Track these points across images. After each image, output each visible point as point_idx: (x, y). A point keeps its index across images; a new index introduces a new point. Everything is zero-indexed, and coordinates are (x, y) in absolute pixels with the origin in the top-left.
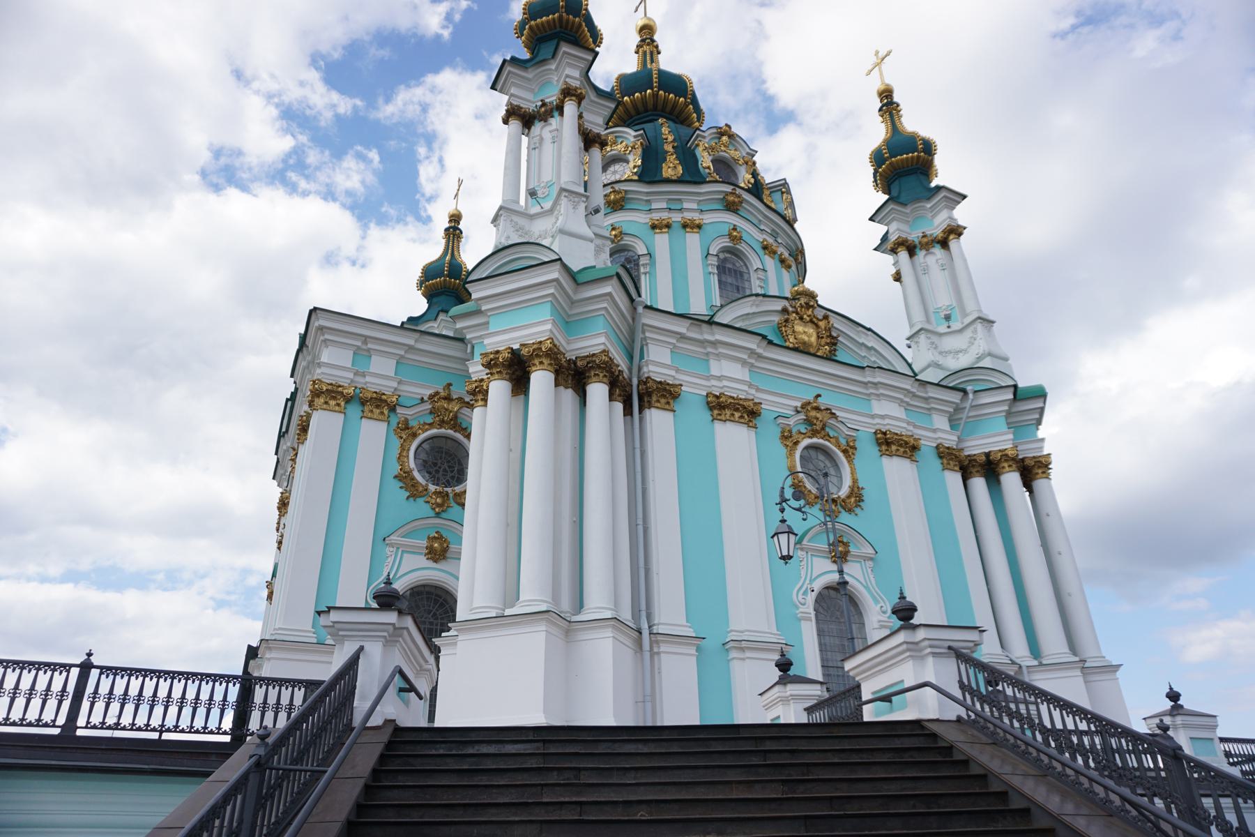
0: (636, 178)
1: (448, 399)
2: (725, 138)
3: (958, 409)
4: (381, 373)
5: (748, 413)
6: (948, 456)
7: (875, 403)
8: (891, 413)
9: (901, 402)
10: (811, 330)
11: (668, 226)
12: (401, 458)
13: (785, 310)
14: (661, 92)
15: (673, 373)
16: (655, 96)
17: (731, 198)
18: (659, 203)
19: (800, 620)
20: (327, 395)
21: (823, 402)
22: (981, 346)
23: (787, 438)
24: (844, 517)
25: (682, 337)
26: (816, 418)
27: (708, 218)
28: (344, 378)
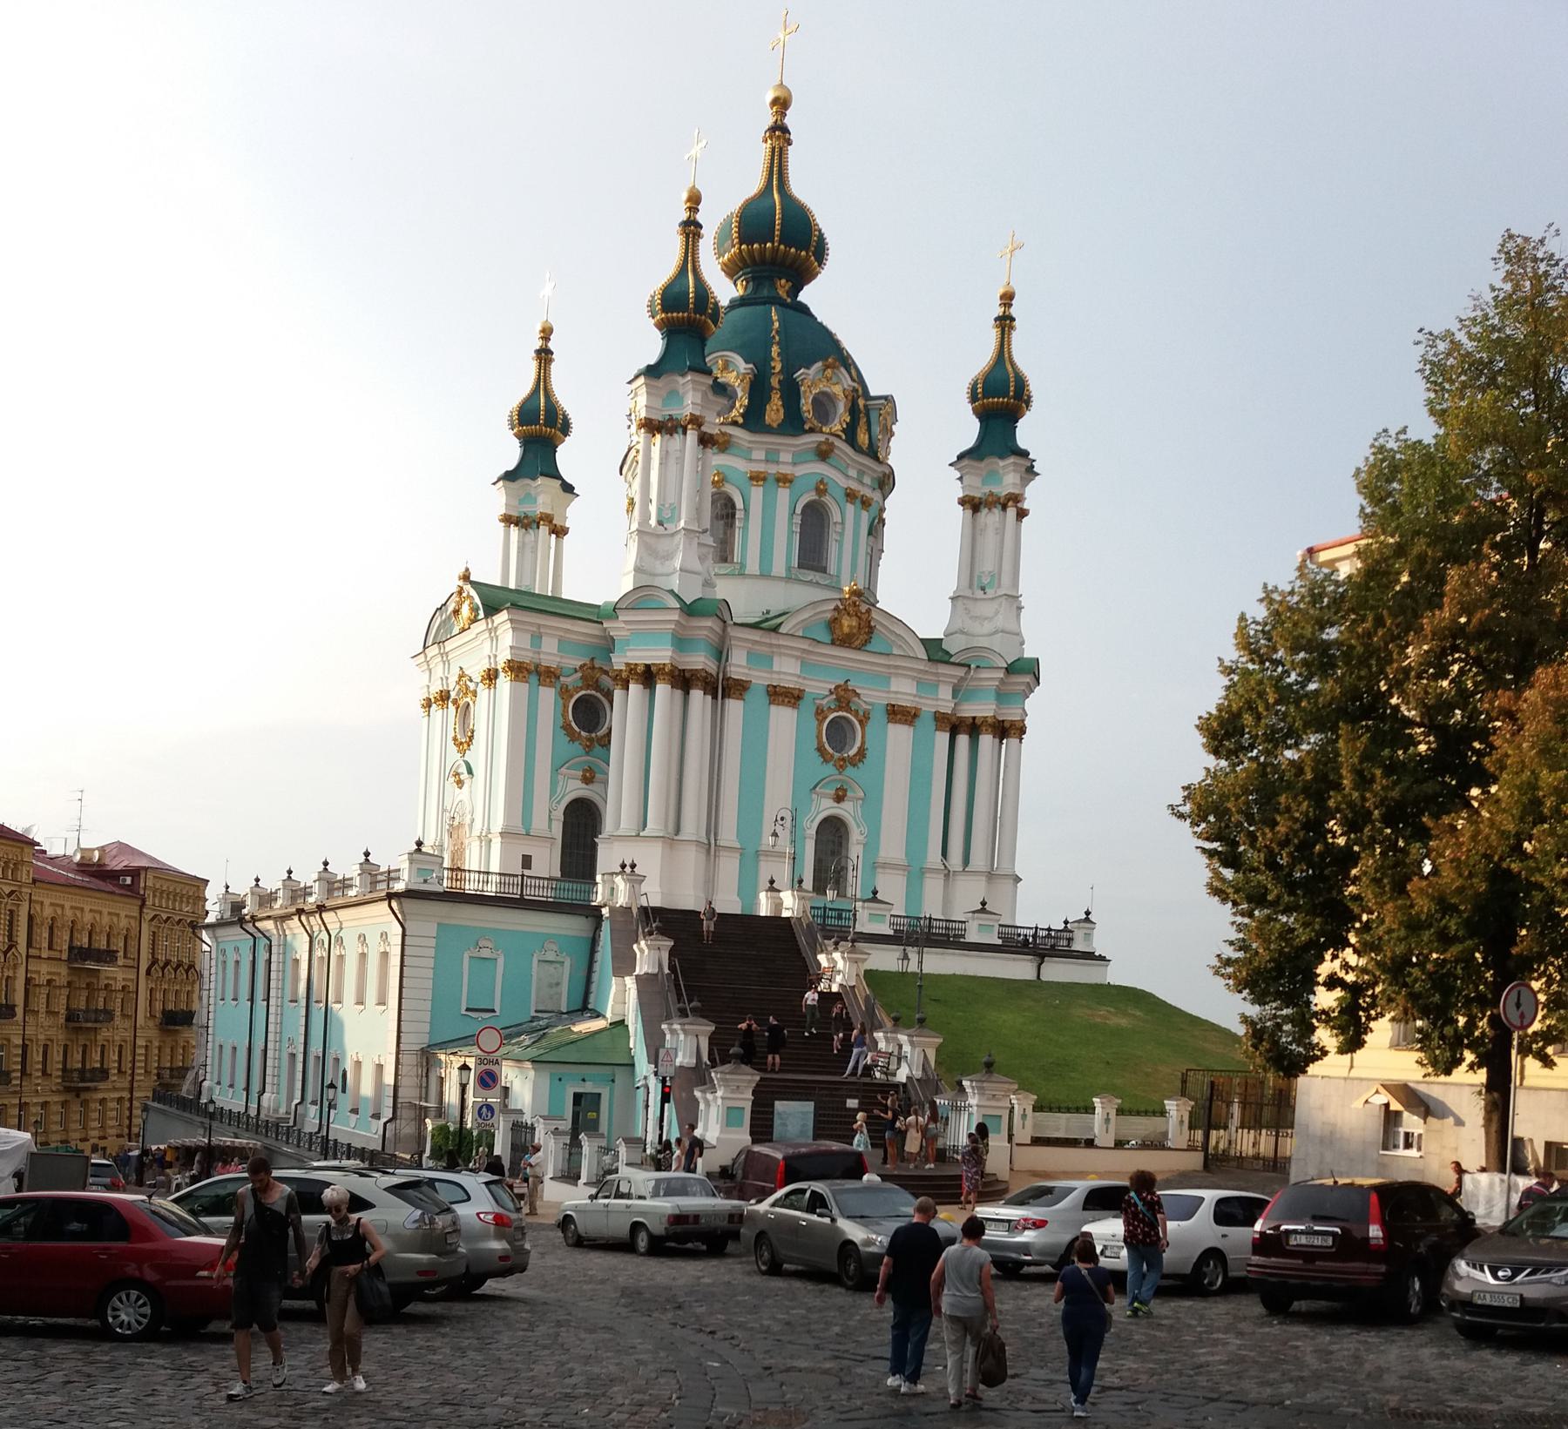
1: (593, 668)
4: (550, 653)
9: (914, 678)
11: (764, 479)
12: (564, 715)
13: (836, 609)
17: (824, 447)
20: (517, 669)
21: (851, 685)
22: (1000, 622)
23: (820, 713)
24: (850, 771)
25: (756, 642)
26: (844, 696)
27: (799, 471)
28: (527, 657)
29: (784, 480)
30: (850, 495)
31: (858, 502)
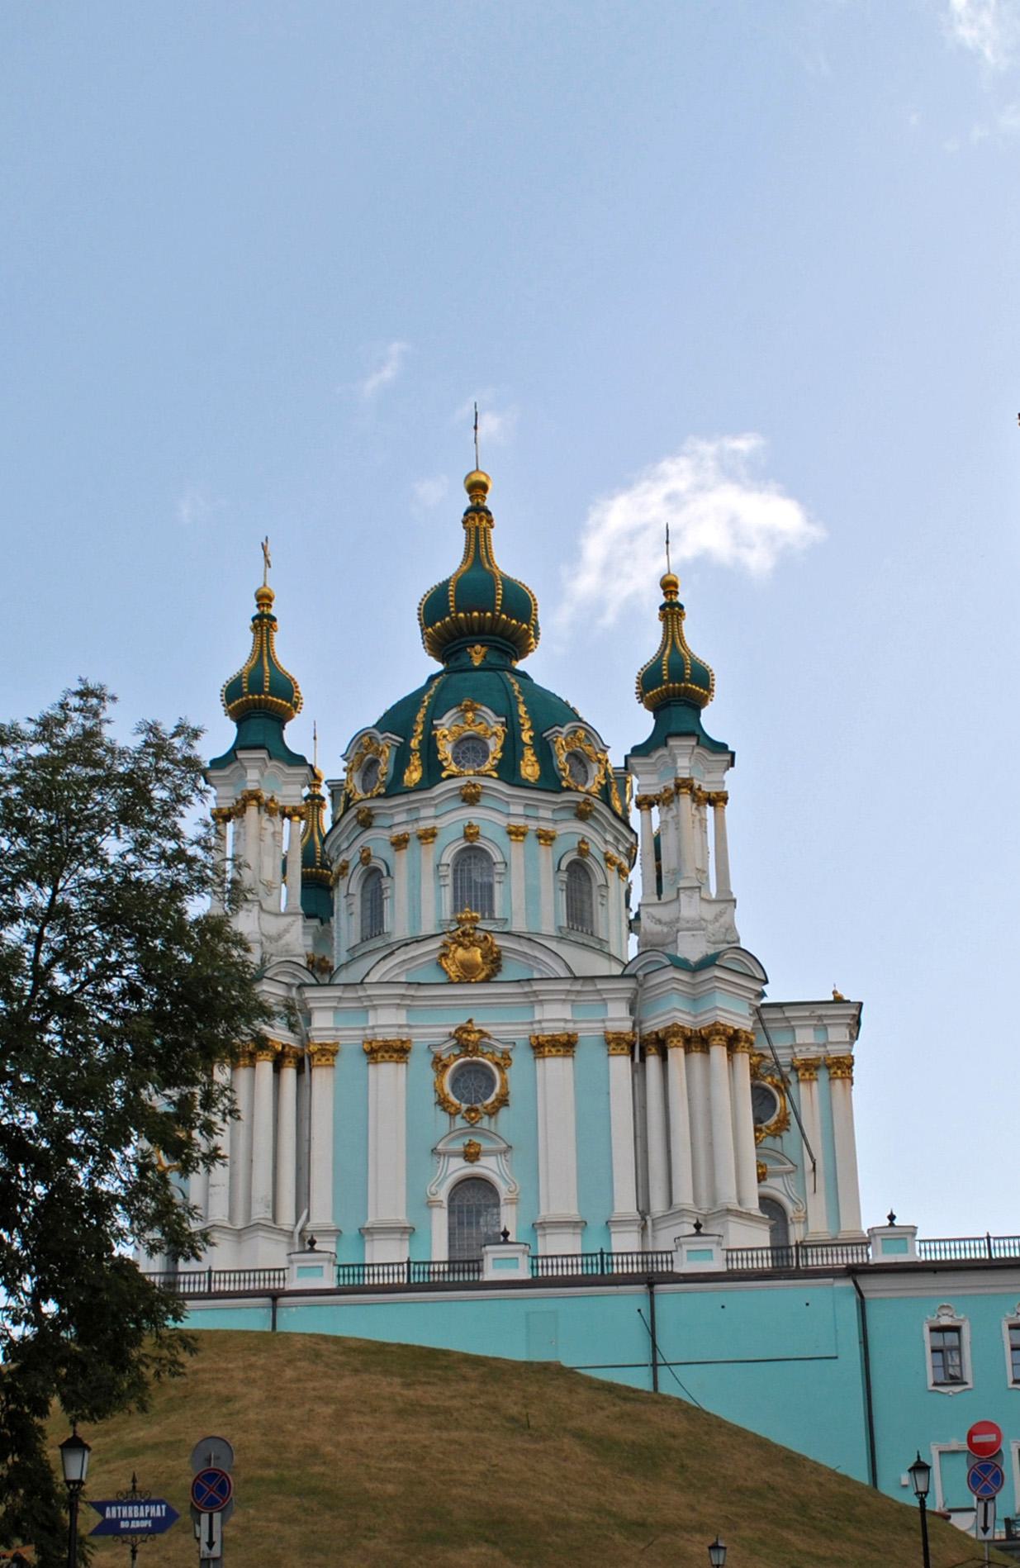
0: (383, 790)
2: (470, 715)
3: (636, 992)
5: (399, 1051)
6: (614, 1042)
7: (537, 1009)
8: (554, 1017)
10: (477, 954)
11: (406, 841)
13: (445, 946)
14: (461, 615)
15: (333, 1033)
16: (456, 620)
18: (397, 817)
19: (430, 1207)
23: (439, 1064)
24: (485, 1123)
26: (465, 1040)
29: (429, 836)
30: (515, 833)
31: (531, 836)
